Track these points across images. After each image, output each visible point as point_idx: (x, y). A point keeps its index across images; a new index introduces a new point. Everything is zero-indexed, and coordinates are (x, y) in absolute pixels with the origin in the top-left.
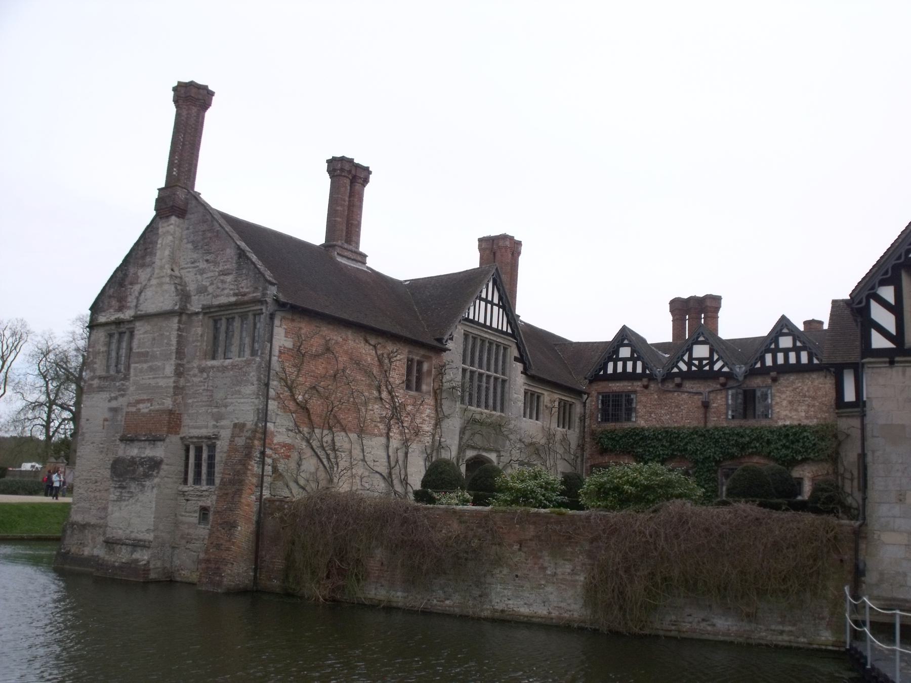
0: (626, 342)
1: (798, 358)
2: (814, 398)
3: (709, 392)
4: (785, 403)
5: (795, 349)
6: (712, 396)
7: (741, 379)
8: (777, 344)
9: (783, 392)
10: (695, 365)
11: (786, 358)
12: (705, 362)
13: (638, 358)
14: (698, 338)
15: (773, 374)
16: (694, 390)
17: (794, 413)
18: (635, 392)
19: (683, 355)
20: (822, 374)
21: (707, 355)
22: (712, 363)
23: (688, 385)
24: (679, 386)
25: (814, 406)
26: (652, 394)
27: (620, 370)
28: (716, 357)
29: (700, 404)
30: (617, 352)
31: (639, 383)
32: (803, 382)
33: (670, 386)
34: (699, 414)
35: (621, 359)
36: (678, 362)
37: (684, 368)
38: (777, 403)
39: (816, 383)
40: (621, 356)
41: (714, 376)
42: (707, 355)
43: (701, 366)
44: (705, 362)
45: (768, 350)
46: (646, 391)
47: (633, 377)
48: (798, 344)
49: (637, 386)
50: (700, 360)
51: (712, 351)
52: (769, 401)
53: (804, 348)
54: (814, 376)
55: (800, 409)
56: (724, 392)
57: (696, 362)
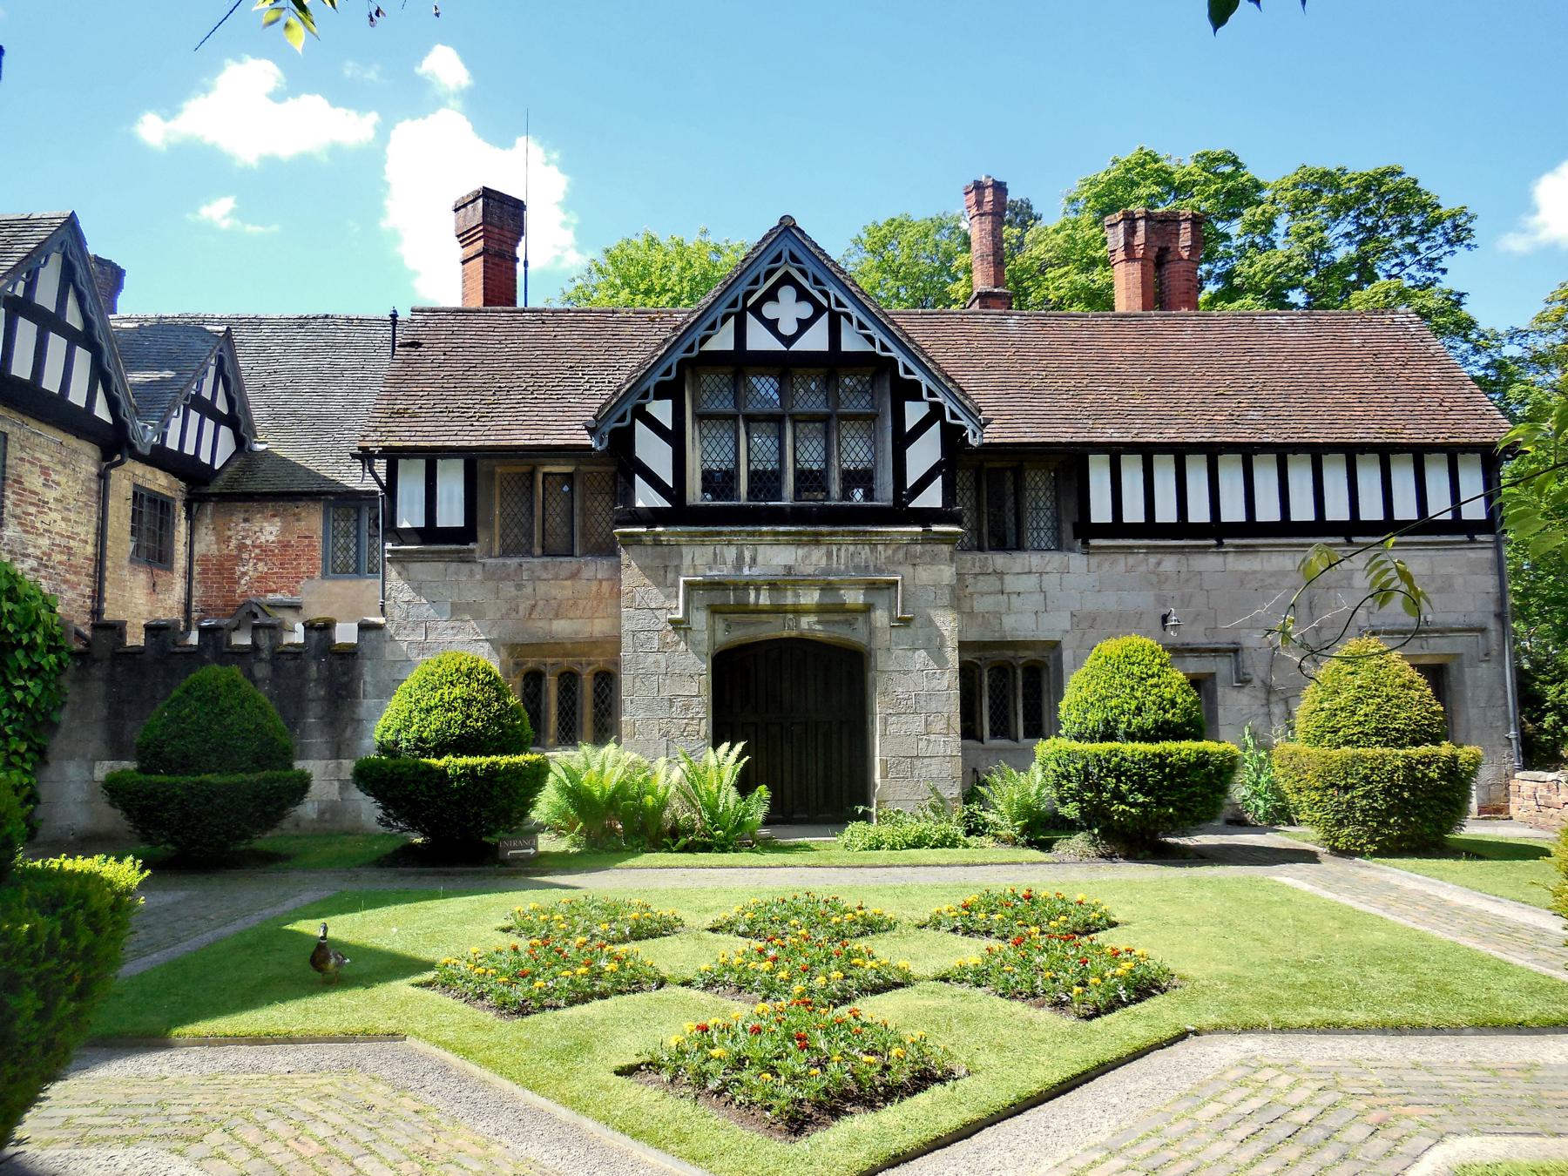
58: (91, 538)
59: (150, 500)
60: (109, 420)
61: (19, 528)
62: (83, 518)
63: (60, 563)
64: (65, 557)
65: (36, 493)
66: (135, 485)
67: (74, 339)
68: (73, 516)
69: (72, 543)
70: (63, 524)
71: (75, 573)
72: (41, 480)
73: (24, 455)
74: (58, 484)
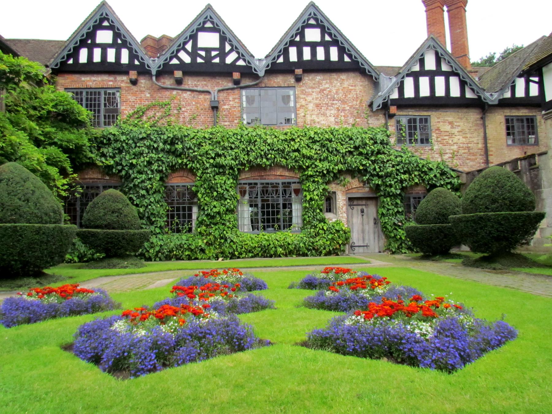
0: (106, 24)
1: (327, 54)
2: (344, 102)
3: (219, 91)
4: (311, 106)
5: (323, 43)
6: (223, 95)
7: (261, 74)
8: (302, 35)
9: (309, 94)
10: (201, 57)
11: (314, 53)
12: (214, 53)
13: (125, 44)
14: (204, 23)
15: (299, 71)
16: (199, 88)
17: (321, 118)
18: (118, 88)
19: (185, 43)
20: (352, 75)
21: (217, 45)
22: (223, 54)
23: (190, 82)
24: (179, 82)
25: (344, 110)
26: (142, 92)
27: (97, 58)
28: (228, 48)
29: (207, 105)
30: (92, 35)
31: (125, 78)
32: (331, 83)
33: (168, 82)
34: (205, 117)
35: (99, 46)
36: (178, 51)
37: (187, 59)
38: (302, 106)
39: (346, 84)
40: (99, 40)
41: (225, 71)
42: (217, 45)
43: (208, 58)
44: (214, 53)
45: (292, 43)
46: (134, 88)
47: (115, 69)
48: (327, 38)
49: (122, 80)
50: (208, 50)
51: (223, 39)
52: (292, 104)
53: (335, 42)
54: (343, 76)
55: (328, 113)
56: (236, 91)
57: (203, 53)
58: (481, 141)
59: (518, 120)
60: (476, 97)
61: (440, 145)
62: (475, 135)
63: (464, 153)
64: (466, 151)
65: (448, 132)
66: (505, 116)
67: (447, 75)
68: (468, 135)
69: (469, 145)
70: (464, 140)
71: (474, 155)
72: (450, 126)
73: (439, 120)
74: (459, 126)
